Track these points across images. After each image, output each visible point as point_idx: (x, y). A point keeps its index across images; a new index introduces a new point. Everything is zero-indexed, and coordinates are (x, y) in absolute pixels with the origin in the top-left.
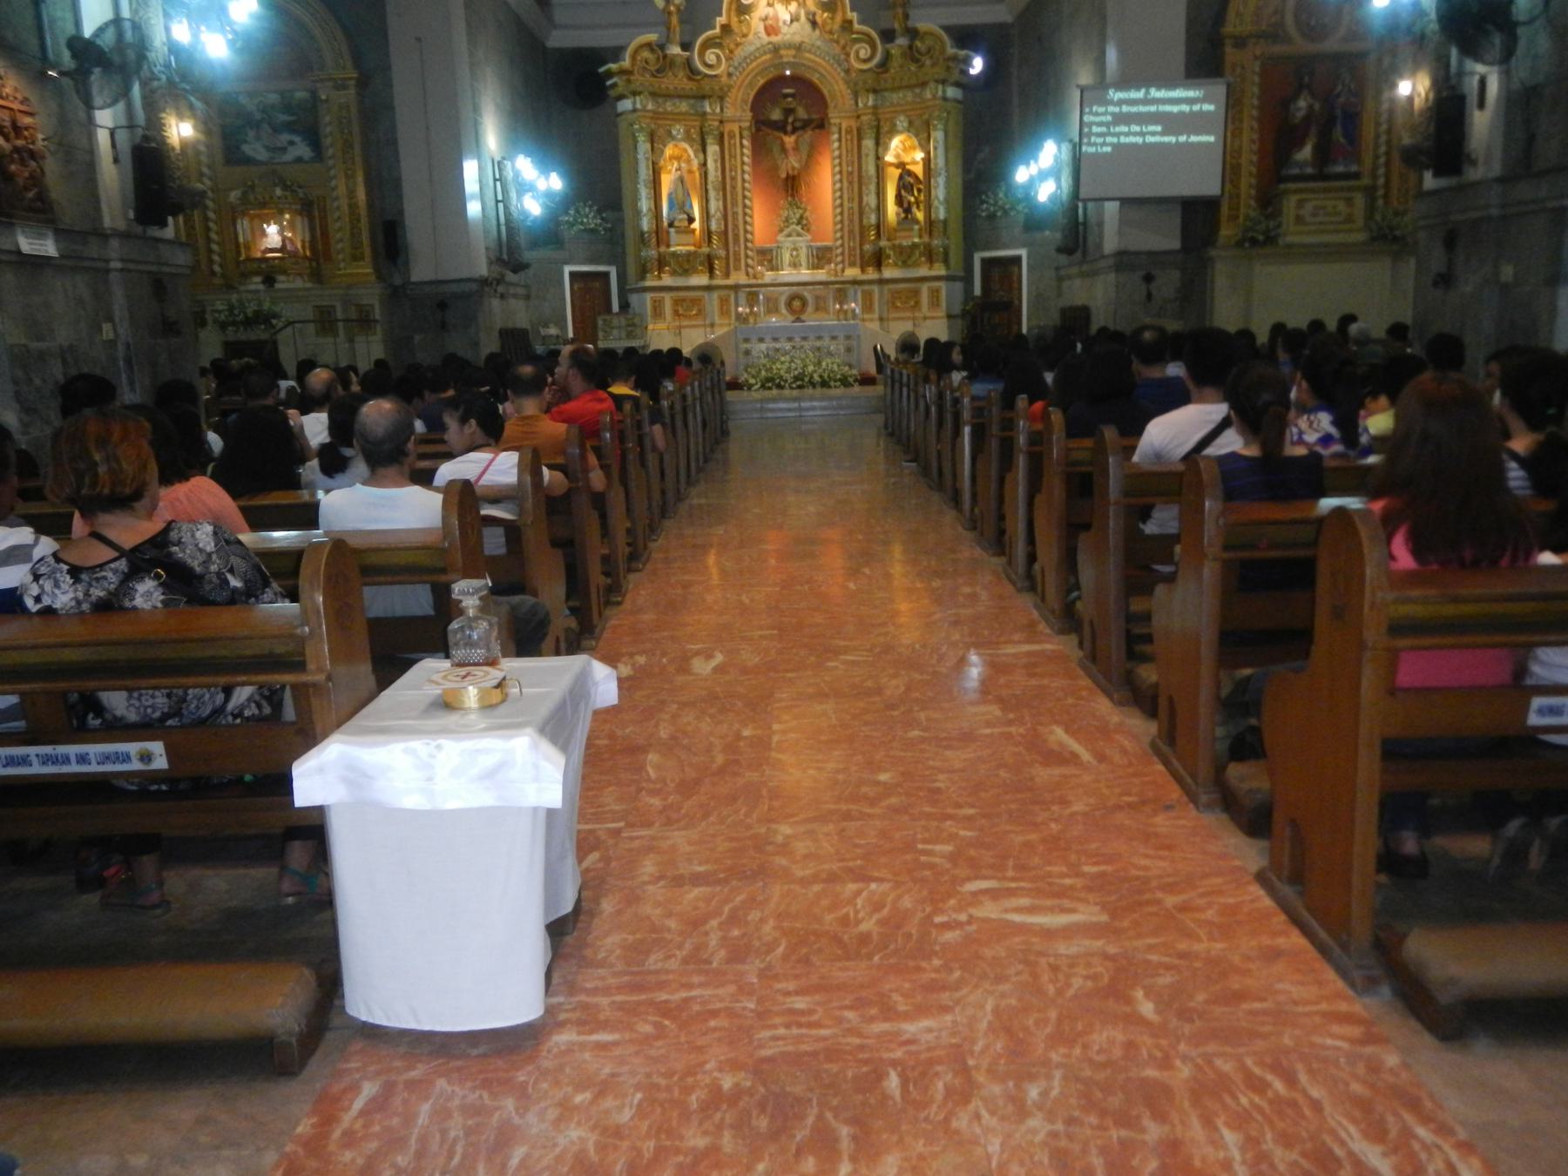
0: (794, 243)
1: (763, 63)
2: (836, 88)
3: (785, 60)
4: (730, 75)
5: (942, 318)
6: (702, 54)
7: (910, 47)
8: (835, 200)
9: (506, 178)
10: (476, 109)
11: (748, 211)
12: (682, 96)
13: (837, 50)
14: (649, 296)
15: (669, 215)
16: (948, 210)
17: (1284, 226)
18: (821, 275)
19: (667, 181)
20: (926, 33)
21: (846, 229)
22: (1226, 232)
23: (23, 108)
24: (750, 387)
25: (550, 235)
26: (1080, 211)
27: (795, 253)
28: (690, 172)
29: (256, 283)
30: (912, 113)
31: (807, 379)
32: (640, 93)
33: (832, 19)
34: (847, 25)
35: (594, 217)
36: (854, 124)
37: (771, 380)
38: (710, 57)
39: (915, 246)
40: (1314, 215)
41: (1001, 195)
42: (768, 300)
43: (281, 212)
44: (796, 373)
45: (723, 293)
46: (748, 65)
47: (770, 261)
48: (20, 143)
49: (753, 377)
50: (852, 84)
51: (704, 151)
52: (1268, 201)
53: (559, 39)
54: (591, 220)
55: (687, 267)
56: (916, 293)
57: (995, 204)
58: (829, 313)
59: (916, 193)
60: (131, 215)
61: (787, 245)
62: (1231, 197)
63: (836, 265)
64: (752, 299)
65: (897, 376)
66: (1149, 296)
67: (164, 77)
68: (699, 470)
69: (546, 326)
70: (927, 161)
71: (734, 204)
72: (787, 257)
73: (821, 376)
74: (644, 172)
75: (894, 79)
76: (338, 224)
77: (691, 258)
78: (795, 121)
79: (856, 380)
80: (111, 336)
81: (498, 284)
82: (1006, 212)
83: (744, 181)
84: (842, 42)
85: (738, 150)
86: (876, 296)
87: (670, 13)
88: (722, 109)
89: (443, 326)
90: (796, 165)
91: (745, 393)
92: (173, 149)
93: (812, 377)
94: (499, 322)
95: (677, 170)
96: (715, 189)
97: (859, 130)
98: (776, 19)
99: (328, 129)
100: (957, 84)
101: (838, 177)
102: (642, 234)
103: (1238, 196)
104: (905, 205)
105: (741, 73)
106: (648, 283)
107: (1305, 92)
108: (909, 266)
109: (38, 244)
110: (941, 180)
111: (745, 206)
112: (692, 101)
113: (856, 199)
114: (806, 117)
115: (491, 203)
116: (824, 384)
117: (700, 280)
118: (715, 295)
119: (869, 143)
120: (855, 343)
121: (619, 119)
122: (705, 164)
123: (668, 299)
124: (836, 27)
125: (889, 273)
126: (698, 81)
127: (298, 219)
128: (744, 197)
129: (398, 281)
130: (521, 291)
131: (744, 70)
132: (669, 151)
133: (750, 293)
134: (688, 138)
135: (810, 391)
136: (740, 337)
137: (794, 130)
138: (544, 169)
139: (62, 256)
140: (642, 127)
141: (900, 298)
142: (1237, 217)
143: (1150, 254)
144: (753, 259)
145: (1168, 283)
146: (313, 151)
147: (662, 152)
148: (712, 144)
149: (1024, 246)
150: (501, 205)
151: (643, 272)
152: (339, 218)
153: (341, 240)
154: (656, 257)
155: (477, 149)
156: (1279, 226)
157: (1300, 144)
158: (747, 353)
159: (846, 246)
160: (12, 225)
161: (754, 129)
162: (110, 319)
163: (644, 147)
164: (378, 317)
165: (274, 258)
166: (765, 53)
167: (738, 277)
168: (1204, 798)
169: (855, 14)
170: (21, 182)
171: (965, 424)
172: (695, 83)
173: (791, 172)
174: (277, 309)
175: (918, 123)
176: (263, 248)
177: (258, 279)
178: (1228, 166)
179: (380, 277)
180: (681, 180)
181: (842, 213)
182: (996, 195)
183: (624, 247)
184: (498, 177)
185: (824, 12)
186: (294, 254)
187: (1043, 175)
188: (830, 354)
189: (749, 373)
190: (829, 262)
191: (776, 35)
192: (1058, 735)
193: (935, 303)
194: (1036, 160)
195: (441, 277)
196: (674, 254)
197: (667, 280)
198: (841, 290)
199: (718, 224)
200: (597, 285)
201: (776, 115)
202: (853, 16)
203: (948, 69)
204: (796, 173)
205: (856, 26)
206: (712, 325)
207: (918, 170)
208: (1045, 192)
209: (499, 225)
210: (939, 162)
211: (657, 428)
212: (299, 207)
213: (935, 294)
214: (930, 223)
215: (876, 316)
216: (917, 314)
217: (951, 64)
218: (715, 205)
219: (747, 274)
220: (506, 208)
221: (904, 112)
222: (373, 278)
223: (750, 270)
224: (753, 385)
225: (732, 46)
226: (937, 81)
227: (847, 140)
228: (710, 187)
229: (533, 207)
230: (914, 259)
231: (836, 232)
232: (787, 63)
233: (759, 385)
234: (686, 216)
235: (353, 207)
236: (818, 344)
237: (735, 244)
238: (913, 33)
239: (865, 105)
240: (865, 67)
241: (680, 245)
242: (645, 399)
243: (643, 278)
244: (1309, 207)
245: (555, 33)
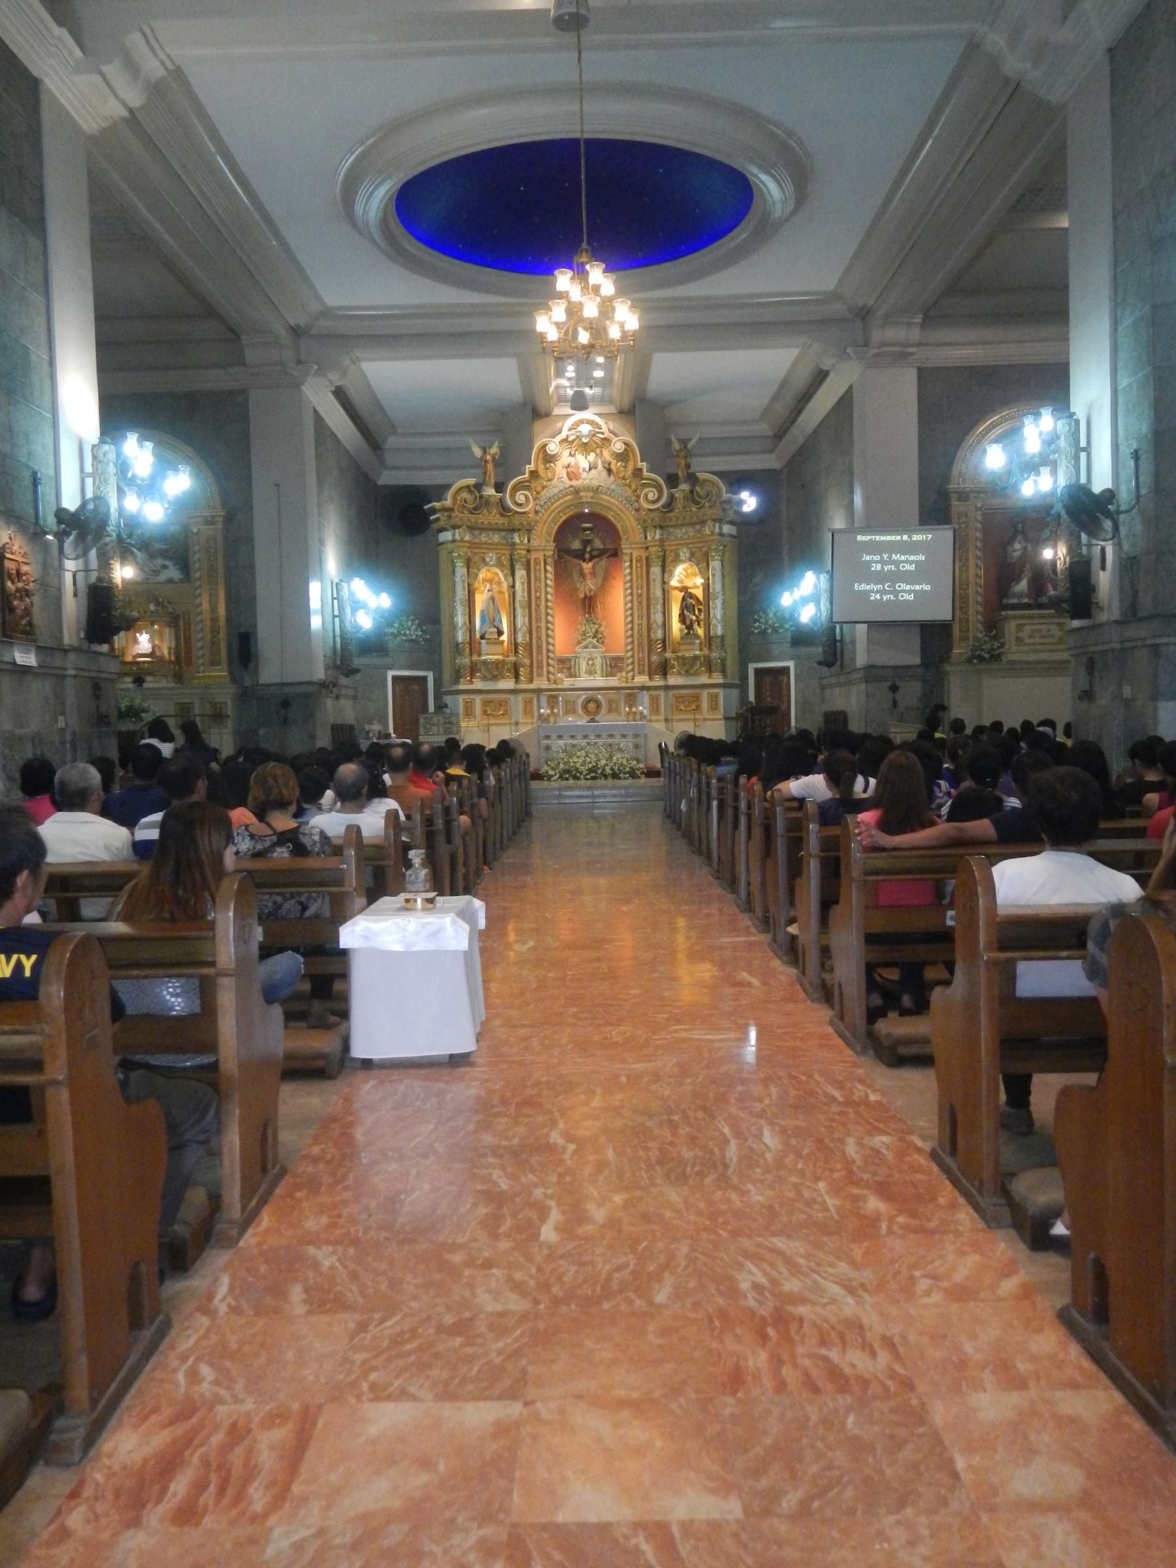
0: (590, 653)
1: (566, 502)
2: (627, 522)
3: (584, 500)
4: (536, 512)
5: (720, 719)
6: (513, 496)
7: (692, 492)
8: (626, 617)
9: (342, 597)
10: (321, 542)
11: (550, 625)
12: (496, 529)
13: (629, 492)
14: (461, 698)
15: (481, 628)
16: (724, 627)
17: (1007, 647)
18: (613, 682)
19: (480, 600)
20: (704, 481)
21: (636, 642)
22: (959, 650)
23: (24, 560)
24: (549, 778)
25: (374, 646)
26: (838, 630)
28: (501, 592)
29: (128, 683)
30: (694, 545)
31: (599, 771)
32: (459, 527)
33: (625, 467)
34: (637, 473)
35: (416, 630)
36: (644, 555)
37: (569, 772)
38: (520, 497)
39: (696, 658)
40: (1030, 637)
41: (771, 615)
42: (566, 702)
43: (153, 624)
44: (590, 766)
45: (529, 695)
46: (552, 505)
47: (570, 668)
48: (20, 585)
49: (553, 769)
51: (513, 574)
52: (993, 626)
53: (387, 478)
54: (414, 632)
55: (495, 673)
56: (697, 698)
57: (766, 623)
58: (620, 715)
59: (697, 613)
60: (82, 635)
61: (584, 655)
62: (960, 619)
63: (627, 672)
64: (553, 701)
65: (672, 766)
66: (895, 703)
67: (114, 534)
68: (510, 840)
69: (370, 723)
70: (706, 587)
71: (538, 620)
72: (584, 665)
73: (612, 769)
74: (461, 593)
75: (677, 519)
76: (200, 635)
77: (500, 666)
78: (592, 550)
79: (643, 773)
80: (63, 726)
81: (334, 686)
82: (775, 630)
83: (547, 600)
84: (634, 486)
86: (662, 701)
87: (486, 462)
88: (529, 541)
89: (285, 721)
90: (593, 587)
91: (545, 783)
92: (117, 587)
93: (604, 770)
94: (332, 719)
95: (489, 591)
96: (521, 607)
97: (647, 559)
98: (577, 466)
99: (197, 556)
100: (732, 523)
102: (457, 644)
103: (967, 621)
104: (688, 622)
105: (546, 511)
106: (461, 687)
107: (1020, 538)
108: (691, 675)
109: (26, 658)
110: (719, 602)
111: (547, 622)
112: (504, 534)
113: (645, 619)
114: (602, 547)
115: (329, 618)
116: (615, 776)
117: (507, 684)
118: (520, 698)
119: (656, 570)
120: (641, 740)
121: (440, 548)
122: (513, 586)
123: (478, 700)
124: (629, 473)
125: (672, 681)
127: (167, 631)
128: (547, 614)
129: (248, 682)
130: (350, 692)
131: (549, 508)
132: (483, 574)
133: (551, 696)
134: (499, 564)
135: (602, 782)
136: (542, 734)
137: (590, 560)
138: (377, 593)
139: (40, 666)
140: (460, 555)
141: (683, 702)
142: (967, 638)
143: (895, 668)
144: (553, 667)
145: (911, 692)
146: (182, 573)
147: (477, 575)
149: (791, 659)
150: (337, 620)
151: (457, 676)
152: (202, 629)
153: (202, 648)
154: (469, 664)
155: (321, 573)
156: (1002, 645)
157: (1018, 579)
158: (548, 748)
159: (636, 656)
160: (12, 643)
161: (556, 557)
162: (63, 713)
163: (461, 571)
164: (229, 714)
165: (144, 662)
166: (568, 495)
167: (540, 683)
168: (815, 996)
169: (644, 463)
170: (19, 612)
171: (713, 799)
173: (588, 593)
174: (146, 705)
175: (698, 554)
176: (134, 653)
177: (129, 679)
178: (957, 596)
179: (234, 679)
180: (493, 599)
181: (632, 629)
182: (767, 615)
183: (440, 655)
184: (335, 596)
185: (618, 461)
186: (161, 659)
187: (805, 601)
188: (620, 750)
189: (549, 766)
190: (621, 670)
192: (745, 975)
193: (714, 707)
194: (798, 589)
195: (285, 681)
196: (485, 662)
197: (478, 684)
198: (632, 695)
199: (524, 636)
200: (416, 688)
201: (576, 545)
202: (644, 466)
203: (724, 510)
204: (592, 593)
205: (645, 473)
206: (517, 724)
207: (699, 593)
209: (334, 637)
210: (717, 586)
211: (483, 801)
212: (168, 619)
213: (713, 699)
214: (709, 639)
215: (662, 717)
216: (698, 717)
217: (727, 507)
218: (521, 621)
219: (549, 680)
220: (342, 622)
221: (686, 544)
222: (228, 680)
223: (551, 676)
224: (552, 776)
225: (539, 489)
226: (713, 520)
228: (517, 605)
229: (365, 622)
230: (695, 669)
231: (627, 645)
232: (587, 503)
233: (558, 775)
234: (495, 630)
235: (214, 620)
236: (610, 741)
238: (692, 479)
239: (653, 538)
240: (656, 506)
241: (490, 655)
242: (474, 777)
243: (456, 681)
244: (1027, 629)
245: (385, 473)
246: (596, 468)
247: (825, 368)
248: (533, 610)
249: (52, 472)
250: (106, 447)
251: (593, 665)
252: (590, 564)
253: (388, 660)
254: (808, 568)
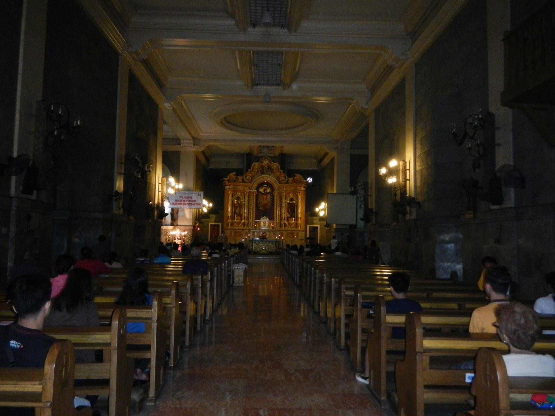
14: (229, 231)
90: (266, 202)
102: (229, 216)
118: (244, 232)
125: (286, 228)
133: (254, 232)
137: (266, 195)
138: (209, 202)
173: (265, 204)
187: (322, 210)
208: (322, 214)
229: (205, 210)
247: (327, 151)
249: (154, 184)
250: (165, 178)
252: (266, 196)
253: (208, 220)
254: (323, 201)
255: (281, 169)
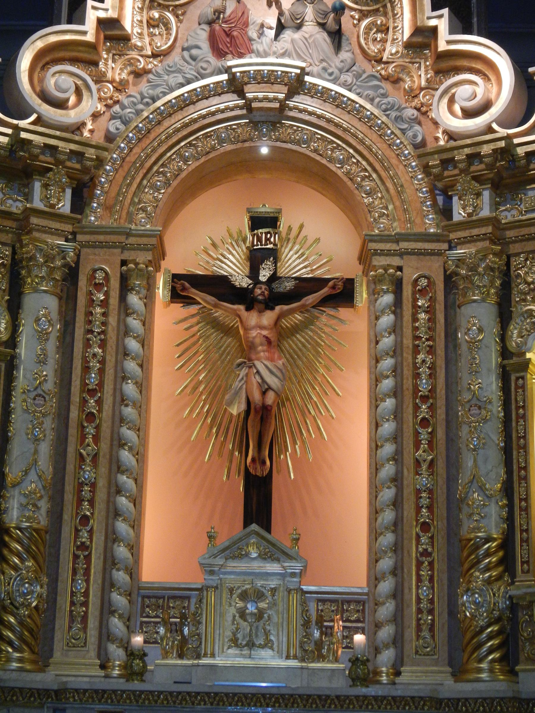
27: (251, 608)
50: (434, 162)
61: (230, 580)
78: (274, 278)
85: (113, 320)
101: (389, 403)
126: (16, 128)
148: (36, 290)
169: (445, 11)
172: (9, 131)
173: (256, 396)
191: (241, 55)
204: (271, 397)
227: (415, 307)
237: (75, 572)
246: (299, 27)
248: (73, 431)
251: (260, 615)
255: (434, 8)
